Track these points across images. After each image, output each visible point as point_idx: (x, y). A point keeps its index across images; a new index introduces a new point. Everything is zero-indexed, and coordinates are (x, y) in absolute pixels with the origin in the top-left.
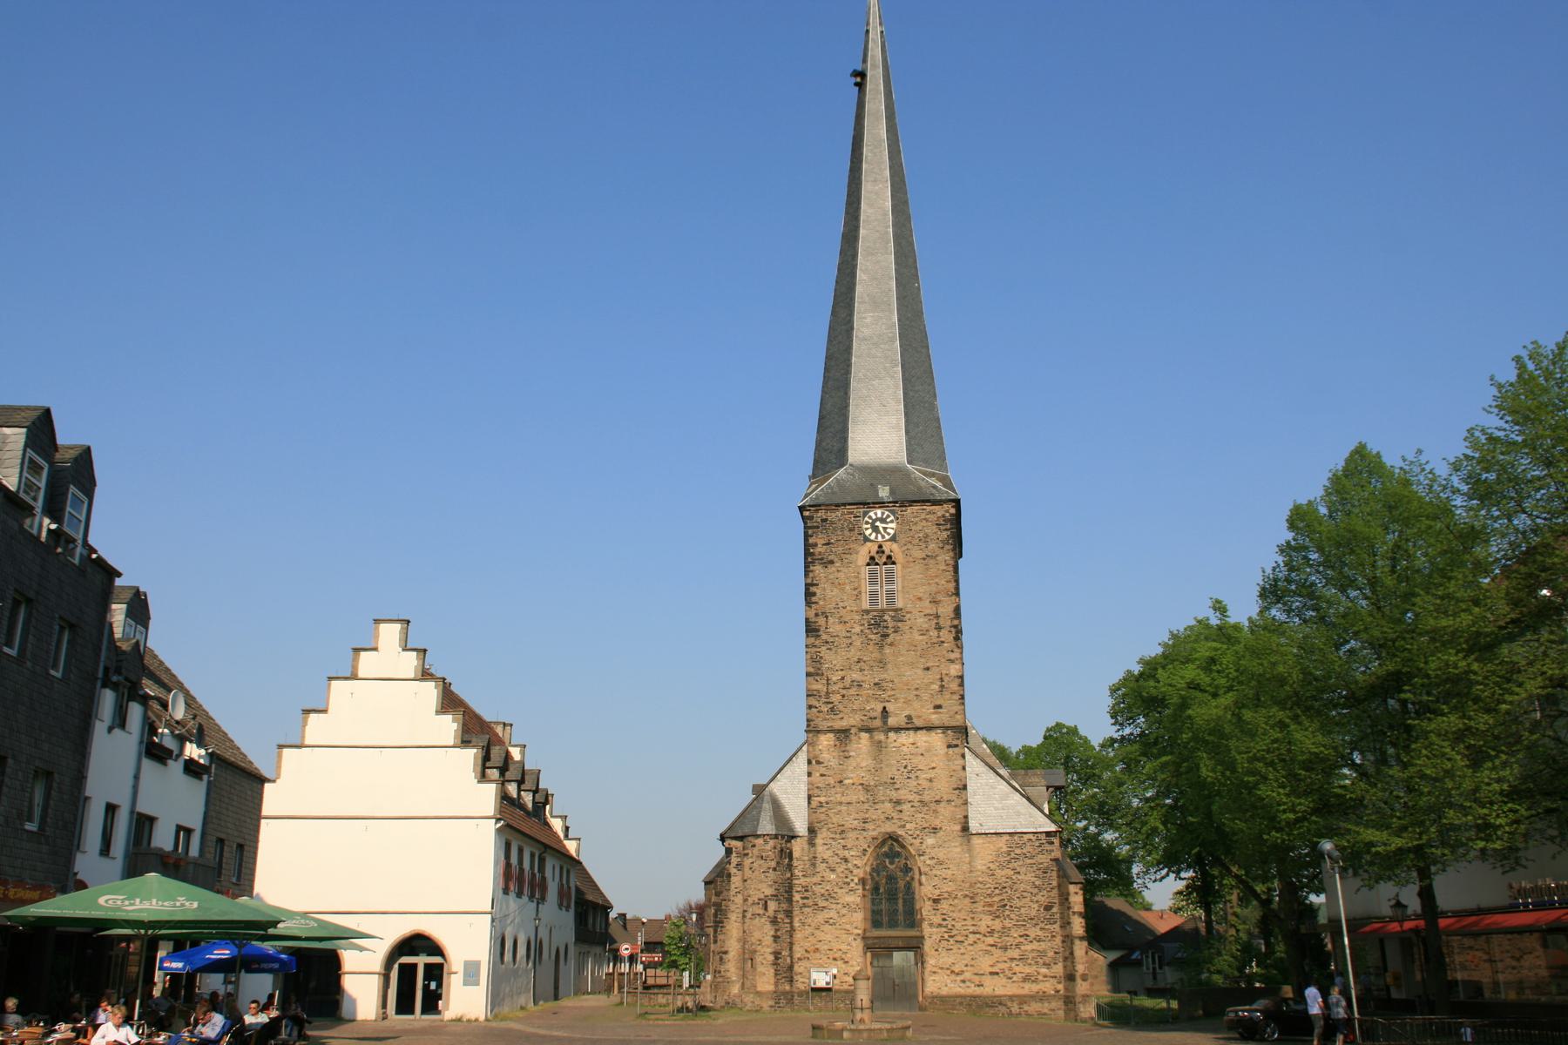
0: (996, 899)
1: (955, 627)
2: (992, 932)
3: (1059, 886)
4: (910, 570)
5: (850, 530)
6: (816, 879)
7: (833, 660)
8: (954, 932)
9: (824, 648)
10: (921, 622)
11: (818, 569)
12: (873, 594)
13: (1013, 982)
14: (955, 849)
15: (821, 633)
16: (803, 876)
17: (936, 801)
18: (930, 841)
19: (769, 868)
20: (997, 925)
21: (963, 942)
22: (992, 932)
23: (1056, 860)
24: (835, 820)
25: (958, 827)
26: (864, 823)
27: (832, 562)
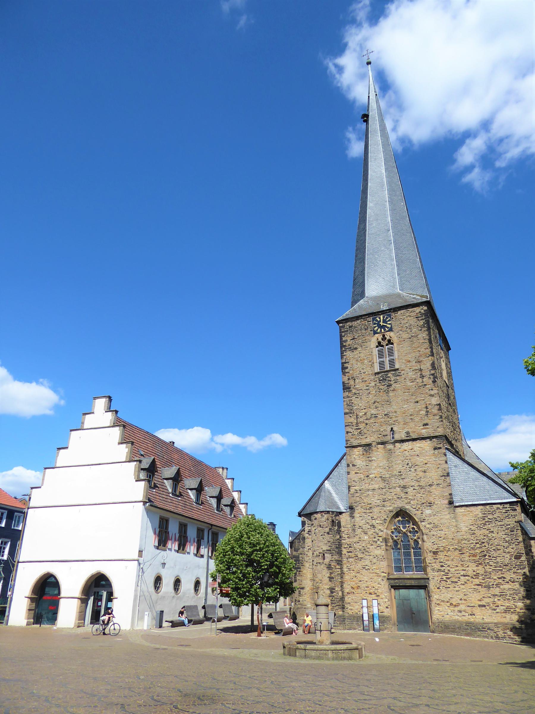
0: (478, 551)
1: (433, 375)
2: (477, 575)
3: (524, 540)
4: (401, 346)
5: (366, 329)
6: (356, 539)
7: (359, 403)
8: (450, 575)
9: (355, 397)
10: (411, 374)
11: (348, 354)
12: (382, 364)
13: (497, 613)
14: (446, 516)
15: (352, 389)
16: (348, 537)
17: (429, 485)
18: (428, 512)
19: (325, 532)
20: (480, 570)
21: (457, 582)
22: (477, 575)
23: (519, 522)
24: (365, 501)
25: (446, 502)
26: (383, 501)
27: (356, 349)
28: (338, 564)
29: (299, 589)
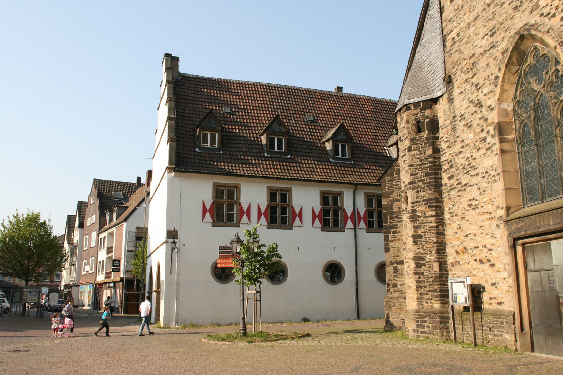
28: (429, 207)
29: (395, 265)
